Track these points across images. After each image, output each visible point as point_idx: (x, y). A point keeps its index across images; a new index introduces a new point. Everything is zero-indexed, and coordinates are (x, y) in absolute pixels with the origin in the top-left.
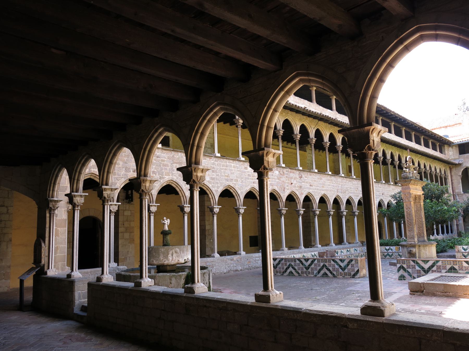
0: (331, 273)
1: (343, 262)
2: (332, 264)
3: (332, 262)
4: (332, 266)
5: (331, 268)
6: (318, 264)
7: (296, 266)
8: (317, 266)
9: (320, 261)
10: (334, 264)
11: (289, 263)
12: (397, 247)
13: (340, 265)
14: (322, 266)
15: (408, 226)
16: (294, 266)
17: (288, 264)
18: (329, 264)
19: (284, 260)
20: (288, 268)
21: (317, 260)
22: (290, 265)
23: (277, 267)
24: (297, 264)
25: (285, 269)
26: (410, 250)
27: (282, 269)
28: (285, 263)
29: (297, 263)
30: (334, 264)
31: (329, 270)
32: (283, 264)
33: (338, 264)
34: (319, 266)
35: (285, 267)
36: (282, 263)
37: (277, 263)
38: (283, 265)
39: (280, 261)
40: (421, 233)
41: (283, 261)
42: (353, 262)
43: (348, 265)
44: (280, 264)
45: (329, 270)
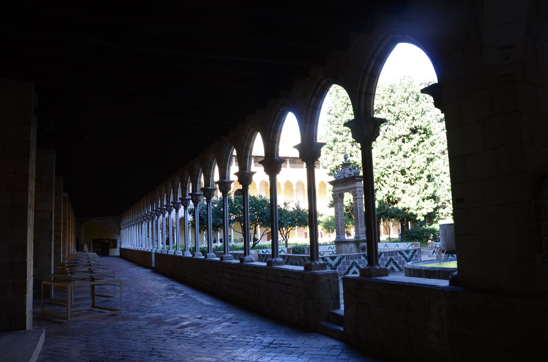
0: (397, 267)
1: (409, 253)
2: (399, 257)
3: (399, 255)
4: (398, 259)
5: (397, 262)
6: (385, 258)
7: (361, 263)
8: (383, 261)
9: (386, 255)
10: (401, 257)
11: (353, 261)
12: (256, 250)
13: (406, 257)
14: (389, 261)
15: (360, 222)
16: (359, 264)
17: (351, 262)
18: (395, 257)
19: (345, 259)
20: (351, 267)
21: (384, 254)
22: (354, 263)
23: (337, 268)
24: (362, 261)
25: (347, 270)
26: (364, 245)
27: (343, 270)
28: (347, 262)
29: (363, 260)
30: (401, 257)
31: (395, 263)
32: (344, 264)
33: (404, 256)
34: (386, 260)
35: (347, 267)
36: (343, 262)
37: (335, 264)
38: (345, 265)
39: (340, 260)
40: (342, 230)
41: (345, 260)
42: (417, 253)
43: (412, 256)
44: (341, 264)
45: (395, 263)
